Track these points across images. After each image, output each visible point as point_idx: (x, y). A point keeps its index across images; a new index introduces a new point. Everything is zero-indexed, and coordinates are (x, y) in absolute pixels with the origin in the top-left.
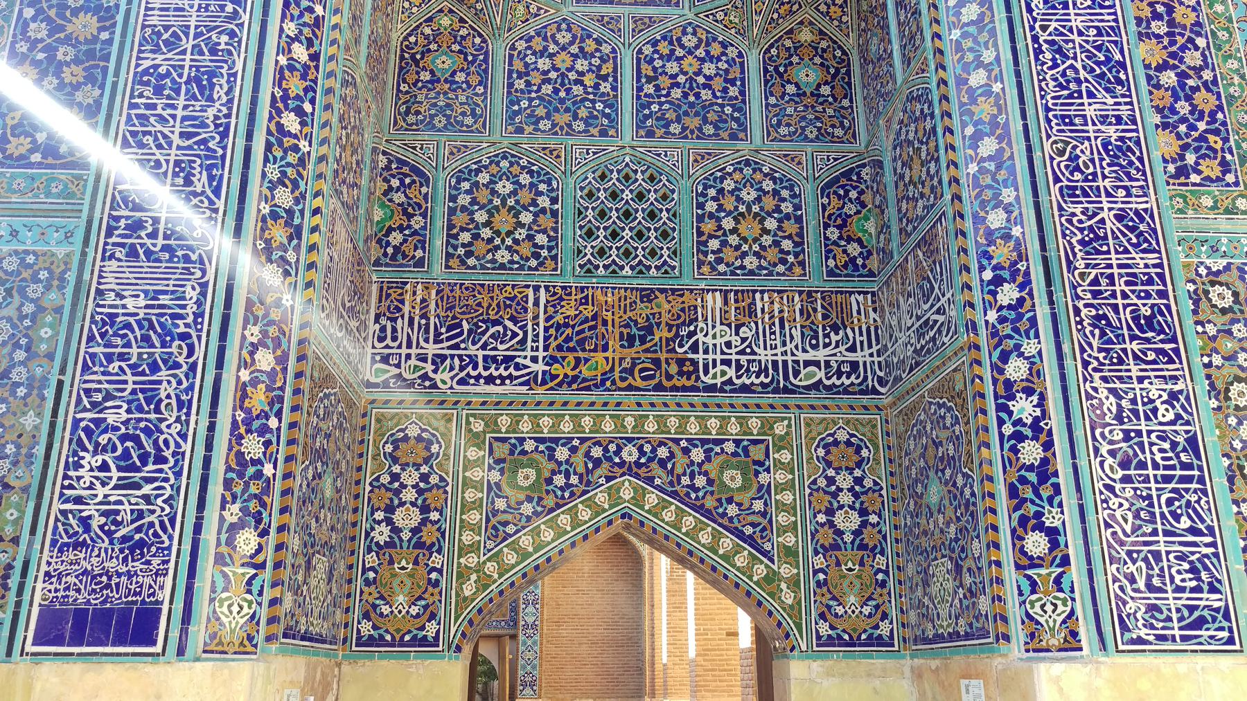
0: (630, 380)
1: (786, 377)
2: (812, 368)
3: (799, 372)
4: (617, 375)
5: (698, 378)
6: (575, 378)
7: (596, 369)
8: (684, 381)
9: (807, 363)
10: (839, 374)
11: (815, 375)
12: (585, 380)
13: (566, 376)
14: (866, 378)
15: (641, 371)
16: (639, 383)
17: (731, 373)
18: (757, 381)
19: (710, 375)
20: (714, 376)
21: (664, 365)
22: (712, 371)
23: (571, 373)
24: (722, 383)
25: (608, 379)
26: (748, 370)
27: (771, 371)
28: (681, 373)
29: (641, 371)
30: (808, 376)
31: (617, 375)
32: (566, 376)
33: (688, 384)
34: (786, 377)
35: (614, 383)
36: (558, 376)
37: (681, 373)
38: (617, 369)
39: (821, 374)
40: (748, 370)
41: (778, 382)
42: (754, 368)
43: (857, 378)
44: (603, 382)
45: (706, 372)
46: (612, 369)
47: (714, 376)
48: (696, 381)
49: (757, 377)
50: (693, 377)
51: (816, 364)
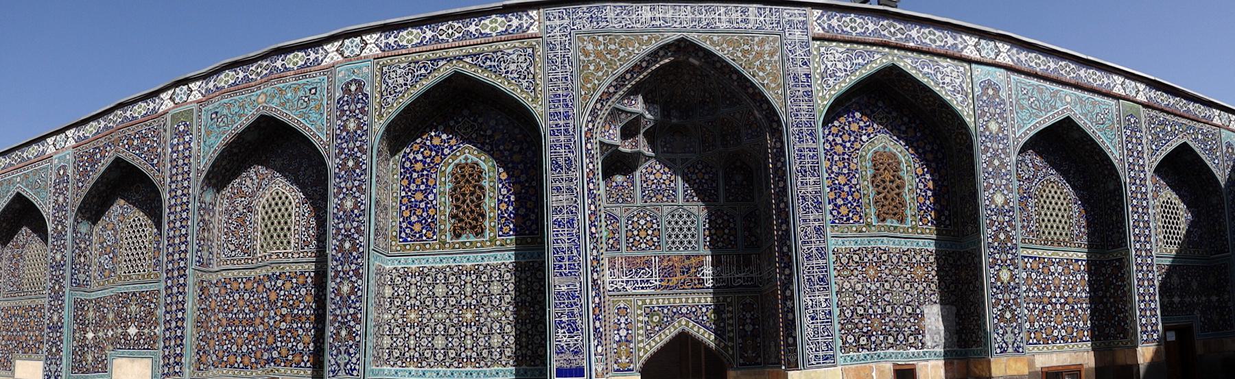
8: (700, 286)
9: (738, 278)
10: (747, 281)
16: (686, 287)
28: (699, 283)
37: (699, 283)
51: (740, 278)
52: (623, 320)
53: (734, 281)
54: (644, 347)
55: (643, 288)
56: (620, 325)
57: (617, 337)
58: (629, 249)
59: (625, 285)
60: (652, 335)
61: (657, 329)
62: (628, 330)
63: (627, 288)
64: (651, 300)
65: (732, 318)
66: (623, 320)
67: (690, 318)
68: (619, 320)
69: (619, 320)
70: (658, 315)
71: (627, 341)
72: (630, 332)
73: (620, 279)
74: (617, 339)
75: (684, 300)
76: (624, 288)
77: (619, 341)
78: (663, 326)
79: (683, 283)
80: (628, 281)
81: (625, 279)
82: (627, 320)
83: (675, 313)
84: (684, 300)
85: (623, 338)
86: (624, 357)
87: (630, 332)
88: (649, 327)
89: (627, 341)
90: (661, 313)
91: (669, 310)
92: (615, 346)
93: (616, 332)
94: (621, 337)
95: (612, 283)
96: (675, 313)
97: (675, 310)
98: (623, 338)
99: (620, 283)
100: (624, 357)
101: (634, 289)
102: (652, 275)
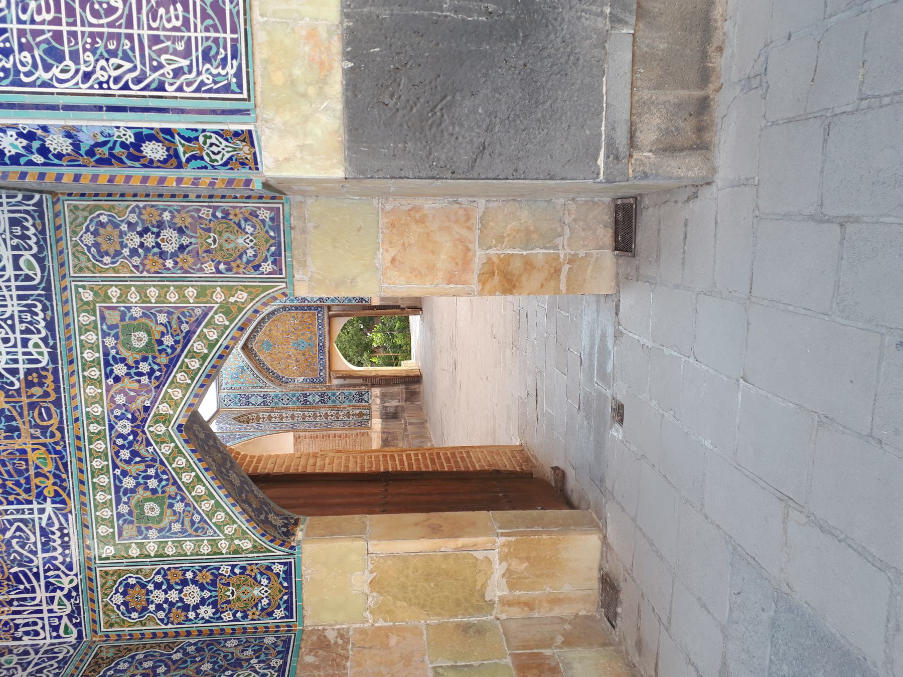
0: (53, 429)
1: (34, 288)
2: (22, 262)
3: (27, 276)
4: (48, 441)
5: (44, 369)
6: (56, 476)
7: (45, 459)
11: (28, 261)
12: (57, 468)
13: (54, 484)
14: (26, 212)
15: (43, 420)
17: (35, 338)
18: (41, 315)
19: (40, 358)
20: (41, 354)
21: (34, 399)
22: (36, 356)
23: (52, 480)
24: (47, 345)
25: (54, 448)
26: (31, 323)
27: (29, 302)
29: (43, 420)
30: (30, 267)
31: (48, 441)
32: (54, 484)
33: (51, 377)
34: (34, 288)
35: (57, 443)
36: (56, 491)
37: (41, 384)
38: (43, 440)
39: (27, 255)
40: (31, 323)
41: (39, 295)
42: (29, 317)
43: (27, 220)
44: (57, 452)
45: (37, 361)
46: (44, 445)
47: (41, 354)
48: (47, 370)
49: (37, 314)
50: (44, 373)
52: (158, 596)
53: (28, 278)
54: (230, 538)
55: (65, 546)
56: (172, 605)
57: (206, 611)
59: (58, 594)
60: (196, 518)
61: (179, 507)
62: (184, 583)
63: (67, 587)
64: (101, 521)
65: (141, 291)
66: (158, 596)
67: (147, 409)
68: (159, 607)
69: (159, 607)
70: (140, 505)
71: (214, 583)
72: (189, 575)
73: (45, 607)
75: (94, 428)
76: (68, 596)
77: (214, 604)
78: (172, 490)
79: (44, 430)
80: (48, 585)
81: (41, 594)
82: (158, 586)
83: (135, 454)
84: (94, 428)
85: (206, 594)
86: (256, 592)
87: (189, 575)
88: (176, 527)
89: (214, 583)
90: (137, 497)
91: (125, 473)
92: (227, 616)
93: (191, 615)
94: (203, 602)
95: (56, 628)
96: (135, 454)
97: (125, 454)
98: (206, 594)
99: (55, 607)
100: (256, 592)
101: (70, 567)
102: (25, 522)
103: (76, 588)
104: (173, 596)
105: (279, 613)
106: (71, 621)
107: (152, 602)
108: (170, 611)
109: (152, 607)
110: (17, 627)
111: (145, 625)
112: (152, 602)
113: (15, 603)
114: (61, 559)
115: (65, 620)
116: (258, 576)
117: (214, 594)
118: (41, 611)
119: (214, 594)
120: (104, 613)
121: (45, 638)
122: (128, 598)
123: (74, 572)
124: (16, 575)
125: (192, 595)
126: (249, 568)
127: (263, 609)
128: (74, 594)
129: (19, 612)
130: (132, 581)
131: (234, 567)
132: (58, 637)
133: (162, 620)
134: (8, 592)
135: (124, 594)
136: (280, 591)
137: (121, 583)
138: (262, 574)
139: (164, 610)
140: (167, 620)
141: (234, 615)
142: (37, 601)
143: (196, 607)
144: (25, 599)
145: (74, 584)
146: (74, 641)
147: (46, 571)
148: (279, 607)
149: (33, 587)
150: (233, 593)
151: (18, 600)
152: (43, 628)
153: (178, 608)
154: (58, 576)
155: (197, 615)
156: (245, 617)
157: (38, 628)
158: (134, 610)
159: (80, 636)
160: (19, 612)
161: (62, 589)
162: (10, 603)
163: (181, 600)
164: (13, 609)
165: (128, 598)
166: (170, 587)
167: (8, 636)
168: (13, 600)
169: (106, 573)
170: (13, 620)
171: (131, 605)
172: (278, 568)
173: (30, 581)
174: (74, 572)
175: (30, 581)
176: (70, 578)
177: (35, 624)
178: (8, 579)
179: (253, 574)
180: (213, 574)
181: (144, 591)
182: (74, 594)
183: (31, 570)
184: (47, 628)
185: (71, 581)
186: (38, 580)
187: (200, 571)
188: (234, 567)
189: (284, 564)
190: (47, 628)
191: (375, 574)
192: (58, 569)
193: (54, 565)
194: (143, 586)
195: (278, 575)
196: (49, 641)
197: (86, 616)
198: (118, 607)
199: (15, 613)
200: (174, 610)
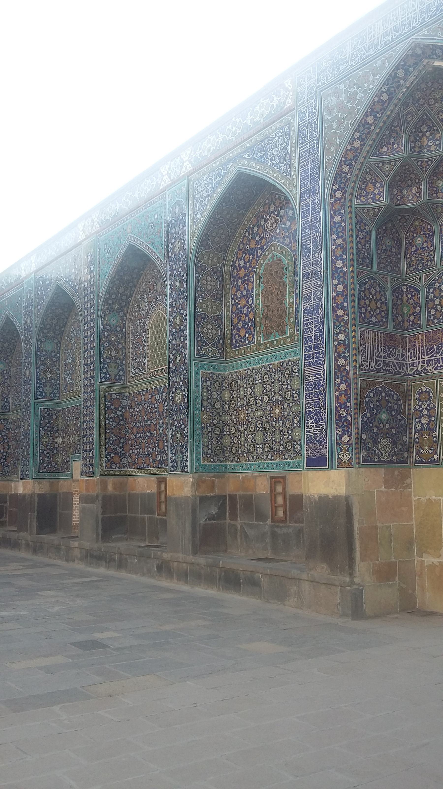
52: (425, 406)
56: (421, 411)
57: (419, 426)
58: (430, 323)
59: (426, 365)
62: (430, 417)
63: (428, 368)
66: (425, 406)
69: (420, 406)
72: (433, 419)
73: (421, 360)
74: (419, 428)
76: (425, 369)
77: (421, 430)
80: (429, 361)
81: (426, 358)
82: (429, 405)
85: (425, 426)
86: (426, 448)
87: (433, 419)
89: (430, 429)
92: (417, 435)
93: (417, 420)
94: (422, 425)
95: (413, 365)
98: (425, 426)
99: (421, 364)
100: (426, 448)
101: (436, 369)
103: (428, 372)
104: (425, 412)
105: (418, 458)
106: (415, 371)
107: (422, 403)
108: (419, 411)
109: (420, 403)
110: (414, 350)
111: (414, 401)
112: (422, 403)
113: (422, 348)
114: (439, 365)
115: (416, 368)
116: (433, 448)
117: (425, 429)
118: (419, 359)
119: (425, 429)
120: (419, 384)
121: (409, 361)
122: (424, 393)
123: (434, 371)
124: (433, 347)
125: (425, 420)
126: (436, 444)
127: (419, 450)
128: (426, 371)
129: (419, 351)
130: (431, 394)
131: (436, 437)
132: (410, 366)
133: (415, 408)
134: (426, 345)
135: (426, 391)
136: (427, 458)
137: (430, 390)
138: (433, 450)
139: (419, 408)
140: (415, 410)
141: (417, 438)
142: (423, 357)
143: (420, 422)
144: (424, 352)
145: (429, 371)
146: (407, 373)
147: (434, 359)
148: (420, 458)
149: (428, 355)
150: (426, 437)
151: (424, 349)
152: (413, 360)
153: (420, 414)
154: (432, 365)
155: (417, 422)
156: (417, 443)
157: (413, 358)
158: (419, 396)
159: (409, 375)
160: (419, 351)
161: (427, 367)
162: (422, 346)
163: (423, 415)
164: (420, 348)
165: (424, 393)
166: (428, 411)
167: (410, 346)
168: (424, 347)
169: (434, 384)
170: (416, 348)
171: (421, 395)
172: (436, 457)
173: (430, 353)
174: (434, 371)
175: (430, 353)
176: (432, 369)
177: (414, 357)
178: (431, 345)
179: (433, 446)
180: (433, 428)
181: (427, 400)
182: (426, 371)
183: (435, 354)
184: (413, 362)
185: (431, 370)
186: (431, 357)
187: (435, 423)
188: (436, 437)
189: (438, 460)
190: (413, 362)
191: (433, 501)
192: (435, 364)
193: (437, 362)
194: (429, 400)
195: (433, 457)
196: (408, 362)
197: (417, 377)
198: (421, 389)
199: (419, 348)
200: (419, 413)
